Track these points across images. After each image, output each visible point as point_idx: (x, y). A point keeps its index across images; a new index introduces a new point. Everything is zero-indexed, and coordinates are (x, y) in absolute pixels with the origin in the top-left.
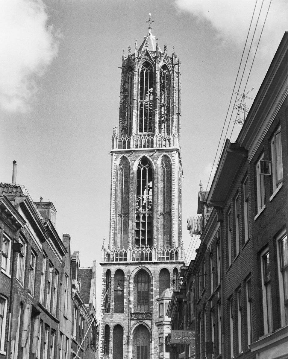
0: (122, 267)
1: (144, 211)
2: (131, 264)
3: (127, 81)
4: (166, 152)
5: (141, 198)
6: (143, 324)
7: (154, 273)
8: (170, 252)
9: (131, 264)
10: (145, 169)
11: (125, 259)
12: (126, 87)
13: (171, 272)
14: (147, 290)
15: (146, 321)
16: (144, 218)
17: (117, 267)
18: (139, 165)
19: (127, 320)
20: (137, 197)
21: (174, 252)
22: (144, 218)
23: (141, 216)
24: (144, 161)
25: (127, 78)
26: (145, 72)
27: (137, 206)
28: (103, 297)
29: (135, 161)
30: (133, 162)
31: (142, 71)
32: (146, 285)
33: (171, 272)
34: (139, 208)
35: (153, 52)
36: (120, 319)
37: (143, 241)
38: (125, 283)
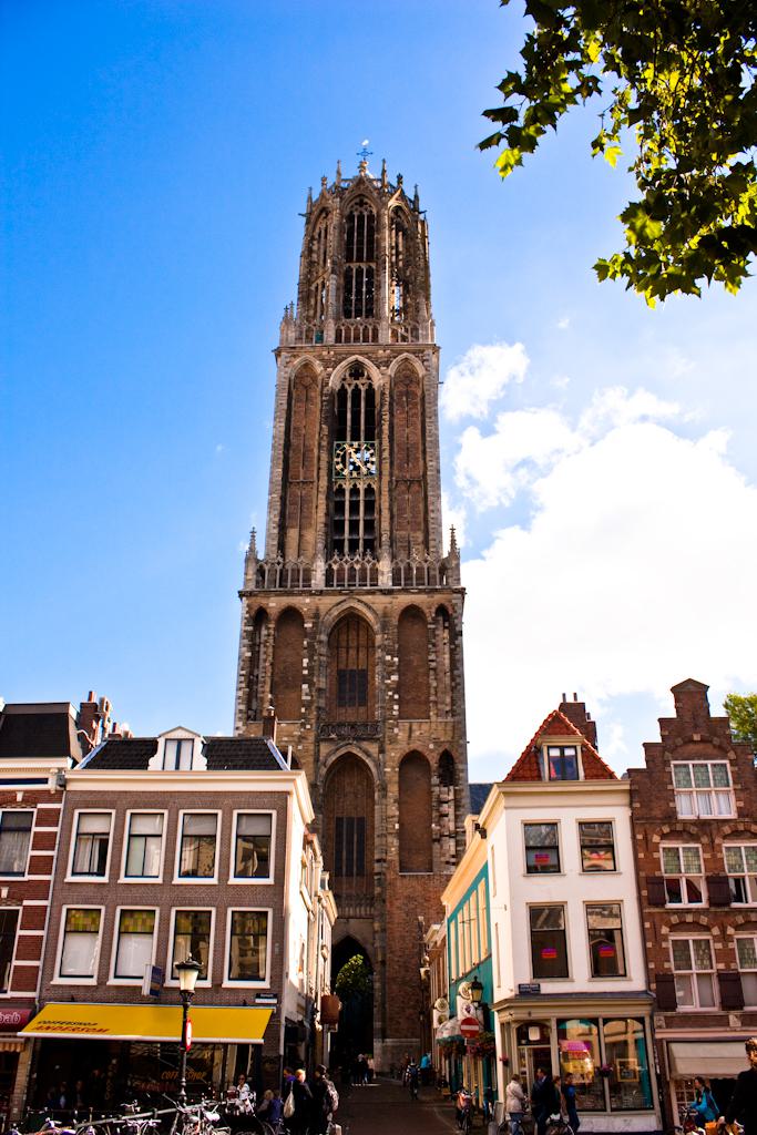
0: (295, 601)
1: (355, 474)
2: (321, 593)
3: (317, 237)
4: (408, 351)
5: (346, 446)
6: (355, 751)
7: (385, 615)
8: (426, 566)
9: (321, 593)
10: (356, 391)
11: (307, 580)
12: (315, 248)
13: (430, 614)
14: (364, 667)
15: (365, 745)
16: (355, 491)
17: (286, 601)
18: (344, 379)
19: (311, 738)
20: (338, 446)
21: (438, 565)
22: (355, 491)
23: (347, 486)
24: (357, 371)
25: (317, 231)
26: (356, 214)
27: (338, 463)
28: (243, 679)
29: (334, 368)
30: (330, 369)
31: (351, 212)
32: (361, 655)
33: (430, 614)
34: (342, 470)
35: (378, 180)
36: (291, 739)
37: (354, 545)
38: (305, 643)
